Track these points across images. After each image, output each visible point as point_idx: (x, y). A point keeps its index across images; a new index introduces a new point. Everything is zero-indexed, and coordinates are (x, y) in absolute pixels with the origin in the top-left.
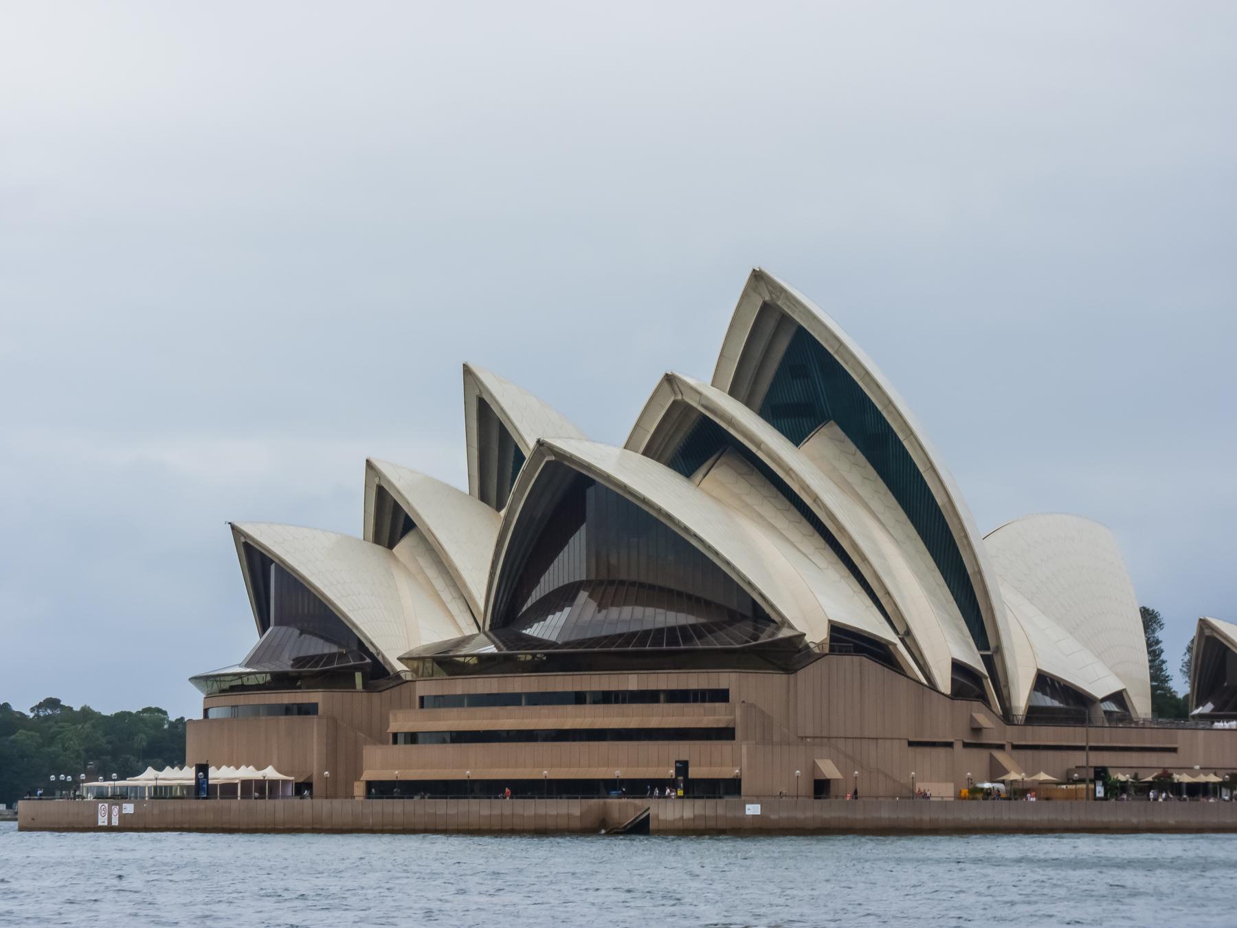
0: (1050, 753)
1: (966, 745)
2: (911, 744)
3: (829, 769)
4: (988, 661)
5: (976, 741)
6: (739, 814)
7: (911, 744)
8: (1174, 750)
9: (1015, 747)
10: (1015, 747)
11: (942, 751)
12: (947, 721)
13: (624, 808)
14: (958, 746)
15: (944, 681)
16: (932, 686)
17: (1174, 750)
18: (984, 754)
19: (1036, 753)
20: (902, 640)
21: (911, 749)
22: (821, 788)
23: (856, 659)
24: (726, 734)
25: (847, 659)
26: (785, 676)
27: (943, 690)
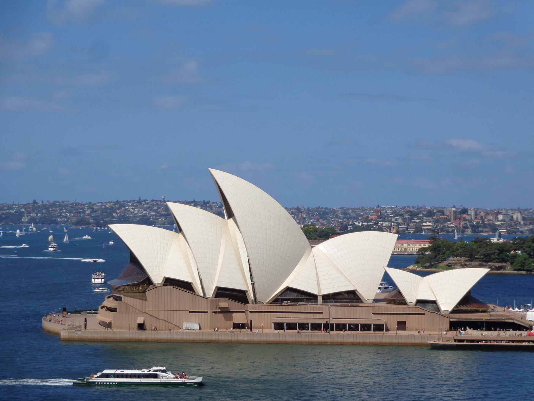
1: (213, 312)
2: (190, 312)
3: (140, 321)
4: (253, 285)
7: (190, 312)
8: (322, 313)
9: (251, 312)
10: (251, 312)
12: (204, 306)
15: (210, 293)
17: (322, 313)
20: (201, 281)
22: (141, 326)
24: (113, 310)
25: (165, 288)
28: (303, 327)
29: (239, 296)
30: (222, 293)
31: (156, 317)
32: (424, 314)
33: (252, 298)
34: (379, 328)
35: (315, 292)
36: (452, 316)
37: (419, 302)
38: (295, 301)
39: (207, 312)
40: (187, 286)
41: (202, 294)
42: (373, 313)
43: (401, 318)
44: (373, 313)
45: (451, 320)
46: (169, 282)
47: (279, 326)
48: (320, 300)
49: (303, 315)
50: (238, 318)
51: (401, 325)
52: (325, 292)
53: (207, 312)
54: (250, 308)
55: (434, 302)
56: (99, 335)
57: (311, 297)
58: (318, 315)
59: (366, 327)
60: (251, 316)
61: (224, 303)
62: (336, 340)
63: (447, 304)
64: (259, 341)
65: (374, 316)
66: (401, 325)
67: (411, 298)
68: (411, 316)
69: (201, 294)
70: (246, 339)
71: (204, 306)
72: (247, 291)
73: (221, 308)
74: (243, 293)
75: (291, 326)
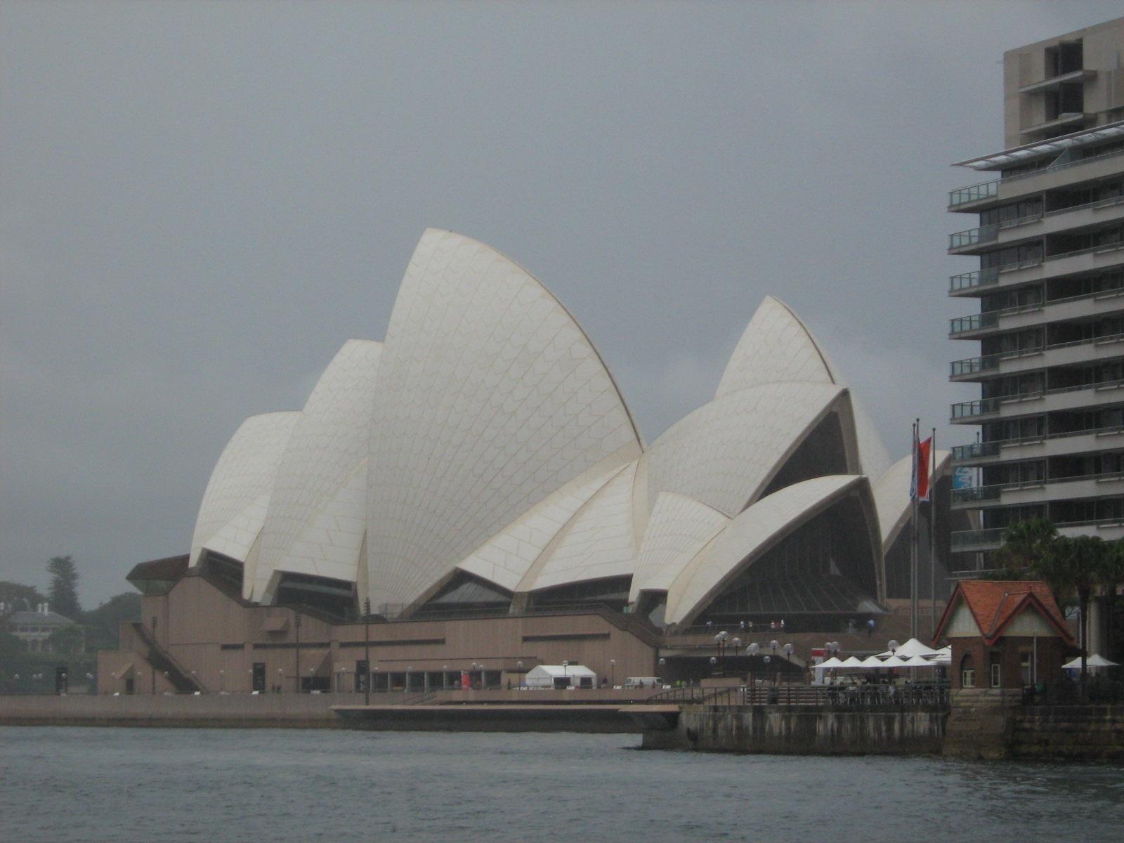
1: (256, 646)
2: (225, 647)
5: (276, 641)
7: (225, 647)
8: (442, 642)
9: (343, 645)
10: (343, 645)
13: (464, 697)
32: (606, 636)
35: (509, 581)
38: (467, 611)
42: (525, 639)
44: (525, 639)
49: (416, 651)
58: (439, 651)
69: (246, 595)
73: (273, 633)
74: (347, 585)
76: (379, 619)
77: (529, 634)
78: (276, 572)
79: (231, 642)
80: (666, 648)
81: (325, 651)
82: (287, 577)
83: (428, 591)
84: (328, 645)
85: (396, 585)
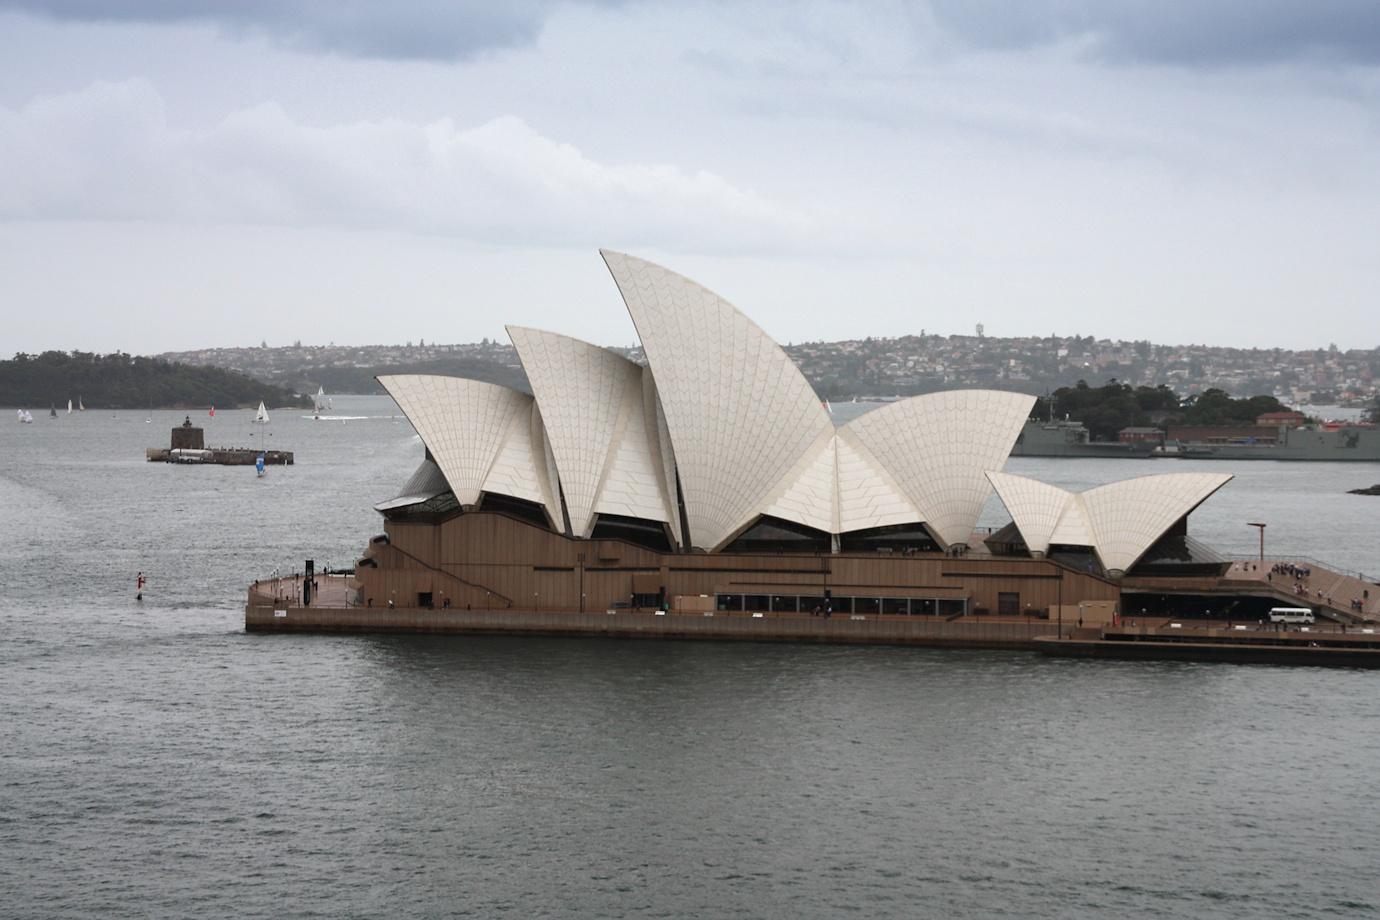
0: (706, 574)
2: (536, 569)
5: (607, 565)
6: (269, 616)
9: (671, 569)
10: (671, 569)
11: (564, 574)
14: (577, 571)
15: (581, 527)
16: (568, 535)
18: (625, 577)
19: (693, 573)
21: (537, 572)
22: (425, 600)
23: (490, 516)
26: (431, 528)
27: (575, 534)
28: (786, 604)
29: (645, 535)
30: (608, 526)
31: (464, 578)
33: (678, 537)
34: (952, 608)
36: (1126, 581)
37: (1055, 549)
39: (572, 569)
40: (530, 513)
41: (561, 529)
42: (944, 575)
43: (1008, 586)
44: (944, 575)
45: (1124, 591)
46: (492, 502)
47: (729, 603)
48: (835, 547)
49: (788, 578)
50: (647, 584)
51: (1009, 605)
52: (849, 526)
53: (572, 569)
54: (668, 560)
55: (1087, 552)
56: (325, 616)
57: (815, 540)
59: (923, 608)
60: (673, 581)
61: (609, 548)
62: (968, 635)
63: (1120, 552)
64: (428, 628)
65: (946, 579)
66: (1009, 605)
67: (1036, 540)
68: (1030, 582)
69: (561, 529)
70: (639, 628)
71: (566, 556)
72: (667, 523)
75: (760, 603)
76: (701, 552)
77: (946, 572)
78: (596, 514)
79: (551, 564)
80: (1132, 587)
81: (658, 573)
82: (602, 516)
83: (738, 531)
84: (658, 569)
85: (715, 522)
